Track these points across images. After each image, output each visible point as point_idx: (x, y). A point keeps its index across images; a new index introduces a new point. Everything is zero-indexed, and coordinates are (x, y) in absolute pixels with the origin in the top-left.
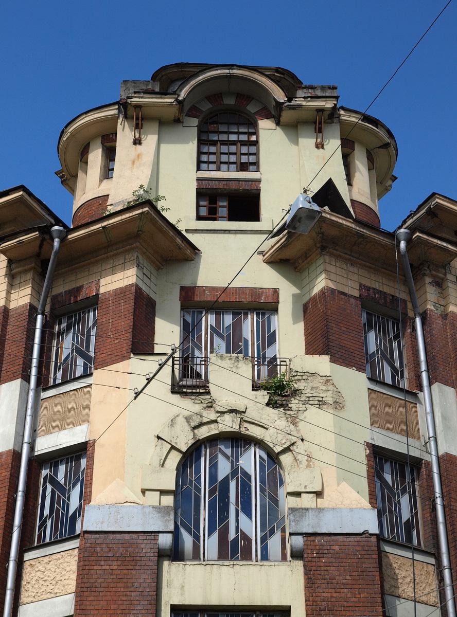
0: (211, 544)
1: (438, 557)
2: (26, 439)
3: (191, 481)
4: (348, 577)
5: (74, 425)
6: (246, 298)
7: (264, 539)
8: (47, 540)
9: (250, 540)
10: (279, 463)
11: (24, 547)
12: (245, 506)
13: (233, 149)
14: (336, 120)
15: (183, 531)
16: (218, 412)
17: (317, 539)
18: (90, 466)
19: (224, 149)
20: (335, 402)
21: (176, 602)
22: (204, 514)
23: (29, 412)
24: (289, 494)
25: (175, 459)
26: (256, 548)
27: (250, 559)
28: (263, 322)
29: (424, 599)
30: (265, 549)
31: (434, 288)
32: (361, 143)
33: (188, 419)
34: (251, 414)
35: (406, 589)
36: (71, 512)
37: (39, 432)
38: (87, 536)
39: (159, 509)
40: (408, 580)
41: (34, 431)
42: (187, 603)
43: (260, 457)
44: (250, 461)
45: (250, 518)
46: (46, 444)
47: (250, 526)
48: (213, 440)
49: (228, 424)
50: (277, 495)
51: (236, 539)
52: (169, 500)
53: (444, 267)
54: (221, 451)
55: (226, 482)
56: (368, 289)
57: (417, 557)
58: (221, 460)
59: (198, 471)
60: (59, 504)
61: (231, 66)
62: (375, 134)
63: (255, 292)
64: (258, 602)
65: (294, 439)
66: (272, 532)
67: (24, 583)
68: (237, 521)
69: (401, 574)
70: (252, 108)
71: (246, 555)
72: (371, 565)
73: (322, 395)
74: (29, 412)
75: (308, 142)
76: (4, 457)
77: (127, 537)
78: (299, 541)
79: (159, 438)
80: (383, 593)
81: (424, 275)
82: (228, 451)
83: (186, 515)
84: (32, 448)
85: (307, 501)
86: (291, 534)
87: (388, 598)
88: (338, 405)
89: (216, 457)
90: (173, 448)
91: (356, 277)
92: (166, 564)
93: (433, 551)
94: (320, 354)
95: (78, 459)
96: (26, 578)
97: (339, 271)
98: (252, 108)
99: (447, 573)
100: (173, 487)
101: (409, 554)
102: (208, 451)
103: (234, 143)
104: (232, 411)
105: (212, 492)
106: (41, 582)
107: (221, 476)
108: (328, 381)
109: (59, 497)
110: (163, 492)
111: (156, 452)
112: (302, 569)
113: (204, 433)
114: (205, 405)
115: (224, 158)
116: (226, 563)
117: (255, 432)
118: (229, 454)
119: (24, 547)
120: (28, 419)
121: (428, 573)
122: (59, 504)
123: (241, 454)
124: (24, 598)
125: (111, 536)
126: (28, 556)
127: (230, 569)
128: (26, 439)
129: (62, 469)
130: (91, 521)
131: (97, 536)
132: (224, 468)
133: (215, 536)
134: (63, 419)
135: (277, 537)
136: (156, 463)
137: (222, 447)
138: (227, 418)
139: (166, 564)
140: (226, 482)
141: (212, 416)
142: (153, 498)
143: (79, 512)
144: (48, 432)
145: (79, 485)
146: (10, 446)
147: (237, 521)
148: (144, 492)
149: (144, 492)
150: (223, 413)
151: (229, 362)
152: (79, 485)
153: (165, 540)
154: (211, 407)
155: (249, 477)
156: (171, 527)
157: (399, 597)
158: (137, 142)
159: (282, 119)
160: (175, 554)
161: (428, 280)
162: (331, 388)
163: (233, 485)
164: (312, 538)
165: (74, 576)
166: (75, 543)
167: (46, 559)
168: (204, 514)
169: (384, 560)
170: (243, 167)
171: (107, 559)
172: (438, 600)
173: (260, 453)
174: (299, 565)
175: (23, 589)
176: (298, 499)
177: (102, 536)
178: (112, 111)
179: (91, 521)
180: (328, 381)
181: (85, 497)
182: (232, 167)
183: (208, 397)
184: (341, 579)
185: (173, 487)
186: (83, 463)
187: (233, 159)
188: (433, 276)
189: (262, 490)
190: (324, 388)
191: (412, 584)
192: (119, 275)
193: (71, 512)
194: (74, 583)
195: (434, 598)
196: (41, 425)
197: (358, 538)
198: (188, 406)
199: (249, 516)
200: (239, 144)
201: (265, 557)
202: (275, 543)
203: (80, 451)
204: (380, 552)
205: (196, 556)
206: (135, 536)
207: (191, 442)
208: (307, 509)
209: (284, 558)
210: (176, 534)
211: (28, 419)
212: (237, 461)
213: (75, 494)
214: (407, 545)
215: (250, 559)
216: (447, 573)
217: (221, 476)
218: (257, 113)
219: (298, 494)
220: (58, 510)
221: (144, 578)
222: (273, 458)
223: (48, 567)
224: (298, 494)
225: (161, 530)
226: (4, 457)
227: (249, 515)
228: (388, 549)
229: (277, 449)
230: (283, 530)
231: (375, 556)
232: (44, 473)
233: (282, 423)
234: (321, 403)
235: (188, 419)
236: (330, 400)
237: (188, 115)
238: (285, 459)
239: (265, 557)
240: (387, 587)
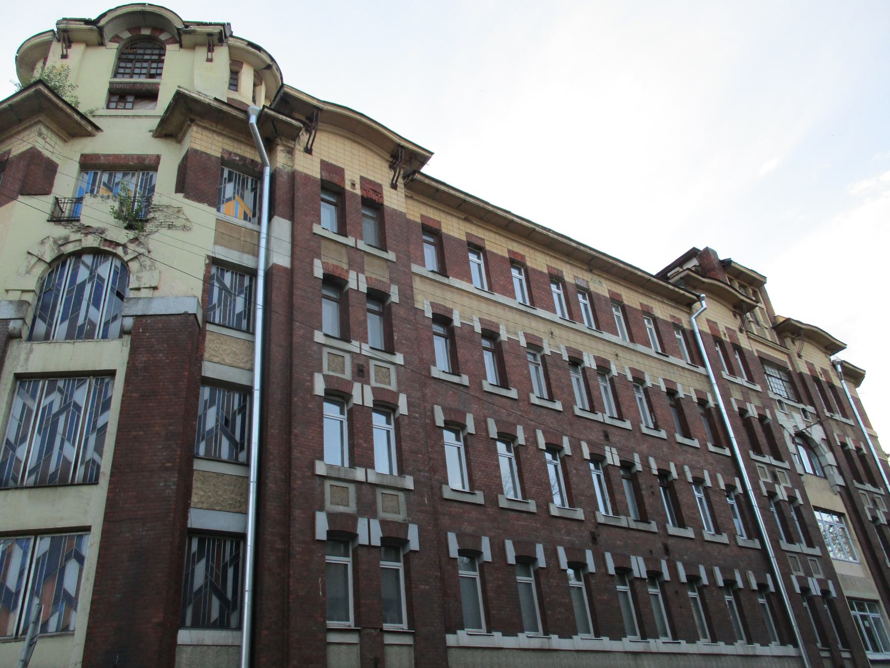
0: (61, 329)
4: (165, 346)
6: (133, 162)
13: (145, 65)
14: (224, 44)
19: (138, 65)
22: (60, 308)
24: (131, 289)
25: (40, 269)
26: (98, 331)
27: (93, 338)
28: (147, 180)
31: (285, 154)
32: (250, 64)
44: (105, 270)
45: (98, 309)
47: (97, 316)
48: (78, 255)
49: (91, 241)
53: (294, 140)
55: (83, 284)
56: (230, 153)
62: (258, 57)
63: (141, 158)
68: (87, 311)
70: (163, 37)
71: (90, 336)
73: (172, 221)
79: (29, 253)
81: (277, 144)
85: (144, 293)
91: (220, 144)
97: (205, 138)
102: (73, 262)
103: (146, 61)
105: (69, 292)
107: (79, 280)
114: (74, 230)
115: (137, 71)
123: (100, 264)
133: (66, 323)
136: (23, 270)
140: (83, 284)
159: (183, 43)
161: (280, 148)
163: (88, 288)
164: (141, 319)
168: (60, 308)
170: (152, 76)
182: (143, 76)
183: (77, 224)
187: (144, 71)
188: (284, 146)
197: (179, 317)
199: (98, 308)
200: (150, 62)
201: (105, 336)
215: (93, 338)
217: (79, 280)
218: (167, 40)
219: (138, 289)
224: (138, 289)
225: (13, 317)
237: (111, 41)
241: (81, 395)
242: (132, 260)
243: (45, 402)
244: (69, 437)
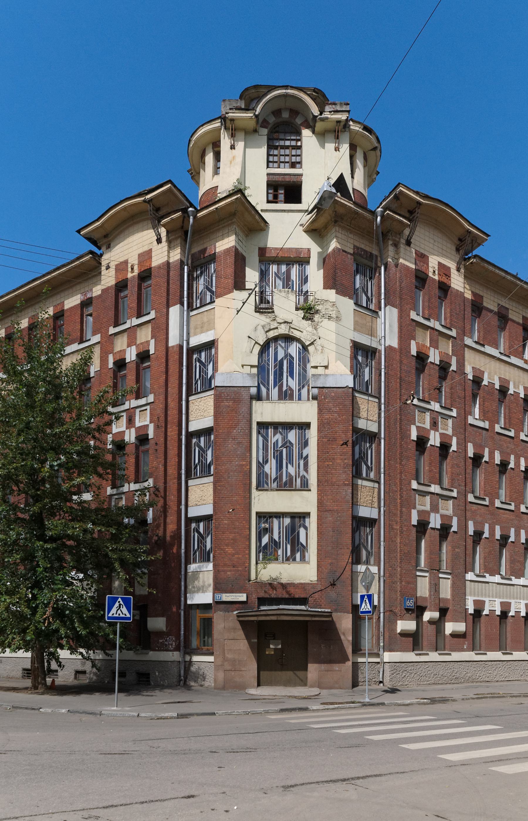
0: (275, 392)
1: (380, 399)
2: (185, 338)
3: (265, 361)
4: (338, 408)
5: (208, 330)
7: (299, 390)
8: (199, 391)
9: (292, 391)
10: (308, 351)
11: (189, 394)
12: (291, 374)
15: (261, 386)
16: (278, 323)
17: (324, 390)
18: (216, 353)
20: (337, 317)
21: (259, 420)
22: (272, 378)
23: (185, 323)
25: (257, 348)
26: (296, 394)
27: (293, 400)
29: (371, 418)
30: (300, 395)
33: (263, 327)
34: (295, 324)
35: (363, 414)
36: (209, 377)
37: (191, 334)
38: (217, 388)
39: (250, 375)
40: (365, 409)
41: (188, 334)
42: (264, 421)
43: (299, 348)
44: (294, 349)
46: (195, 341)
47: (293, 384)
48: (276, 339)
49: (283, 330)
50: (306, 367)
51: (286, 390)
52: (255, 371)
54: (280, 344)
57: (370, 399)
58: (279, 349)
59: (268, 355)
60: (203, 373)
61: (286, 87)
64: (296, 420)
65: (316, 338)
66: (303, 387)
67: (190, 411)
68: (287, 381)
69: (362, 407)
71: (291, 398)
72: (348, 403)
74: (185, 323)
75: (330, 146)
76: (175, 348)
77: (236, 389)
78: (316, 391)
79: (249, 337)
80: (353, 416)
82: (283, 345)
83: (264, 378)
84: (188, 343)
85: (320, 371)
86: (312, 387)
87: (355, 418)
88: (338, 319)
89: (277, 348)
90: (256, 343)
92: (254, 402)
93: (377, 396)
94: (331, 289)
95: (211, 348)
96: (191, 409)
98: (299, 121)
99: (383, 406)
100: (257, 364)
101: (366, 397)
104: (285, 322)
105: (275, 366)
106: (198, 411)
107: (279, 359)
108: (334, 305)
109: (203, 369)
110: (252, 366)
111: (247, 345)
112: (316, 405)
113: (271, 334)
116: (282, 402)
117: (296, 334)
118: (284, 346)
119: (189, 394)
120: (185, 327)
121: (374, 406)
122: (203, 373)
124: (191, 418)
125: (228, 389)
126: (191, 398)
127: (283, 405)
128: (185, 338)
129: (203, 354)
130: (218, 381)
131: (222, 388)
132: (281, 354)
133: (277, 388)
134: (202, 327)
135: (305, 389)
136: (248, 351)
137: (280, 342)
138: (283, 326)
139: (254, 402)
141: (274, 325)
142: (247, 369)
143: (213, 376)
144: (195, 334)
145: (212, 363)
146: (178, 343)
147: (287, 381)
148: (243, 366)
149: (243, 366)
150: (281, 323)
151: (284, 294)
152: (212, 363)
153: (254, 391)
154: (275, 320)
155: (293, 358)
156: (256, 385)
157: (360, 418)
158: (233, 147)
160: (258, 397)
162: (335, 309)
164: (322, 389)
165: (212, 408)
166: (212, 392)
167: (199, 400)
168: (272, 378)
169: (355, 400)
171: (227, 400)
172: (377, 419)
173: (299, 345)
174: (315, 402)
175: (190, 414)
176: (316, 370)
177: (224, 388)
178: (217, 124)
179: (218, 381)
180: (334, 305)
181: (215, 369)
184: (334, 409)
185: (257, 364)
186: (213, 351)
189: (299, 365)
190: (332, 309)
191: (366, 412)
192: (226, 240)
193: (209, 377)
194: (213, 411)
195: (376, 418)
196: (192, 331)
197: (343, 389)
198: (263, 319)
199: (293, 378)
201: (300, 399)
202: (304, 391)
203: (211, 345)
204: (353, 397)
205: (268, 398)
206: (239, 389)
207: (265, 340)
208: (320, 375)
209: (308, 399)
210: (258, 387)
211: (185, 327)
212: (287, 350)
213: (210, 367)
214: (366, 393)
215: (293, 400)
216: (383, 406)
217: (279, 358)
219: (316, 367)
220: (203, 376)
221: (244, 409)
222: (305, 348)
223: (200, 403)
224: (316, 367)
226: (175, 348)
227: (293, 378)
228: (357, 395)
229: (307, 343)
230: (309, 386)
231: (351, 398)
232: (195, 356)
233: (310, 329)
234: (330, 318)
235: (263, 327)
236: (334, 316)
238: (311, 349)
239: (300, 399)
240: (355, 413)
241: (292, 436)
242: (310, 345)
243: (274, 440)
244: (290, 460)
